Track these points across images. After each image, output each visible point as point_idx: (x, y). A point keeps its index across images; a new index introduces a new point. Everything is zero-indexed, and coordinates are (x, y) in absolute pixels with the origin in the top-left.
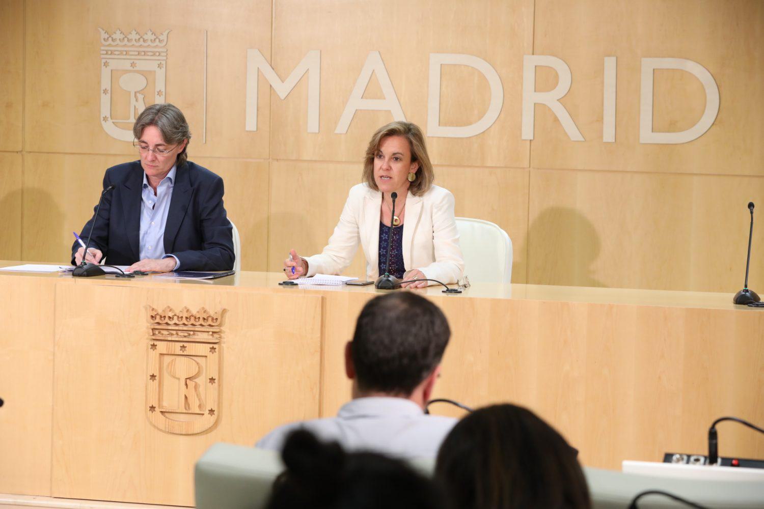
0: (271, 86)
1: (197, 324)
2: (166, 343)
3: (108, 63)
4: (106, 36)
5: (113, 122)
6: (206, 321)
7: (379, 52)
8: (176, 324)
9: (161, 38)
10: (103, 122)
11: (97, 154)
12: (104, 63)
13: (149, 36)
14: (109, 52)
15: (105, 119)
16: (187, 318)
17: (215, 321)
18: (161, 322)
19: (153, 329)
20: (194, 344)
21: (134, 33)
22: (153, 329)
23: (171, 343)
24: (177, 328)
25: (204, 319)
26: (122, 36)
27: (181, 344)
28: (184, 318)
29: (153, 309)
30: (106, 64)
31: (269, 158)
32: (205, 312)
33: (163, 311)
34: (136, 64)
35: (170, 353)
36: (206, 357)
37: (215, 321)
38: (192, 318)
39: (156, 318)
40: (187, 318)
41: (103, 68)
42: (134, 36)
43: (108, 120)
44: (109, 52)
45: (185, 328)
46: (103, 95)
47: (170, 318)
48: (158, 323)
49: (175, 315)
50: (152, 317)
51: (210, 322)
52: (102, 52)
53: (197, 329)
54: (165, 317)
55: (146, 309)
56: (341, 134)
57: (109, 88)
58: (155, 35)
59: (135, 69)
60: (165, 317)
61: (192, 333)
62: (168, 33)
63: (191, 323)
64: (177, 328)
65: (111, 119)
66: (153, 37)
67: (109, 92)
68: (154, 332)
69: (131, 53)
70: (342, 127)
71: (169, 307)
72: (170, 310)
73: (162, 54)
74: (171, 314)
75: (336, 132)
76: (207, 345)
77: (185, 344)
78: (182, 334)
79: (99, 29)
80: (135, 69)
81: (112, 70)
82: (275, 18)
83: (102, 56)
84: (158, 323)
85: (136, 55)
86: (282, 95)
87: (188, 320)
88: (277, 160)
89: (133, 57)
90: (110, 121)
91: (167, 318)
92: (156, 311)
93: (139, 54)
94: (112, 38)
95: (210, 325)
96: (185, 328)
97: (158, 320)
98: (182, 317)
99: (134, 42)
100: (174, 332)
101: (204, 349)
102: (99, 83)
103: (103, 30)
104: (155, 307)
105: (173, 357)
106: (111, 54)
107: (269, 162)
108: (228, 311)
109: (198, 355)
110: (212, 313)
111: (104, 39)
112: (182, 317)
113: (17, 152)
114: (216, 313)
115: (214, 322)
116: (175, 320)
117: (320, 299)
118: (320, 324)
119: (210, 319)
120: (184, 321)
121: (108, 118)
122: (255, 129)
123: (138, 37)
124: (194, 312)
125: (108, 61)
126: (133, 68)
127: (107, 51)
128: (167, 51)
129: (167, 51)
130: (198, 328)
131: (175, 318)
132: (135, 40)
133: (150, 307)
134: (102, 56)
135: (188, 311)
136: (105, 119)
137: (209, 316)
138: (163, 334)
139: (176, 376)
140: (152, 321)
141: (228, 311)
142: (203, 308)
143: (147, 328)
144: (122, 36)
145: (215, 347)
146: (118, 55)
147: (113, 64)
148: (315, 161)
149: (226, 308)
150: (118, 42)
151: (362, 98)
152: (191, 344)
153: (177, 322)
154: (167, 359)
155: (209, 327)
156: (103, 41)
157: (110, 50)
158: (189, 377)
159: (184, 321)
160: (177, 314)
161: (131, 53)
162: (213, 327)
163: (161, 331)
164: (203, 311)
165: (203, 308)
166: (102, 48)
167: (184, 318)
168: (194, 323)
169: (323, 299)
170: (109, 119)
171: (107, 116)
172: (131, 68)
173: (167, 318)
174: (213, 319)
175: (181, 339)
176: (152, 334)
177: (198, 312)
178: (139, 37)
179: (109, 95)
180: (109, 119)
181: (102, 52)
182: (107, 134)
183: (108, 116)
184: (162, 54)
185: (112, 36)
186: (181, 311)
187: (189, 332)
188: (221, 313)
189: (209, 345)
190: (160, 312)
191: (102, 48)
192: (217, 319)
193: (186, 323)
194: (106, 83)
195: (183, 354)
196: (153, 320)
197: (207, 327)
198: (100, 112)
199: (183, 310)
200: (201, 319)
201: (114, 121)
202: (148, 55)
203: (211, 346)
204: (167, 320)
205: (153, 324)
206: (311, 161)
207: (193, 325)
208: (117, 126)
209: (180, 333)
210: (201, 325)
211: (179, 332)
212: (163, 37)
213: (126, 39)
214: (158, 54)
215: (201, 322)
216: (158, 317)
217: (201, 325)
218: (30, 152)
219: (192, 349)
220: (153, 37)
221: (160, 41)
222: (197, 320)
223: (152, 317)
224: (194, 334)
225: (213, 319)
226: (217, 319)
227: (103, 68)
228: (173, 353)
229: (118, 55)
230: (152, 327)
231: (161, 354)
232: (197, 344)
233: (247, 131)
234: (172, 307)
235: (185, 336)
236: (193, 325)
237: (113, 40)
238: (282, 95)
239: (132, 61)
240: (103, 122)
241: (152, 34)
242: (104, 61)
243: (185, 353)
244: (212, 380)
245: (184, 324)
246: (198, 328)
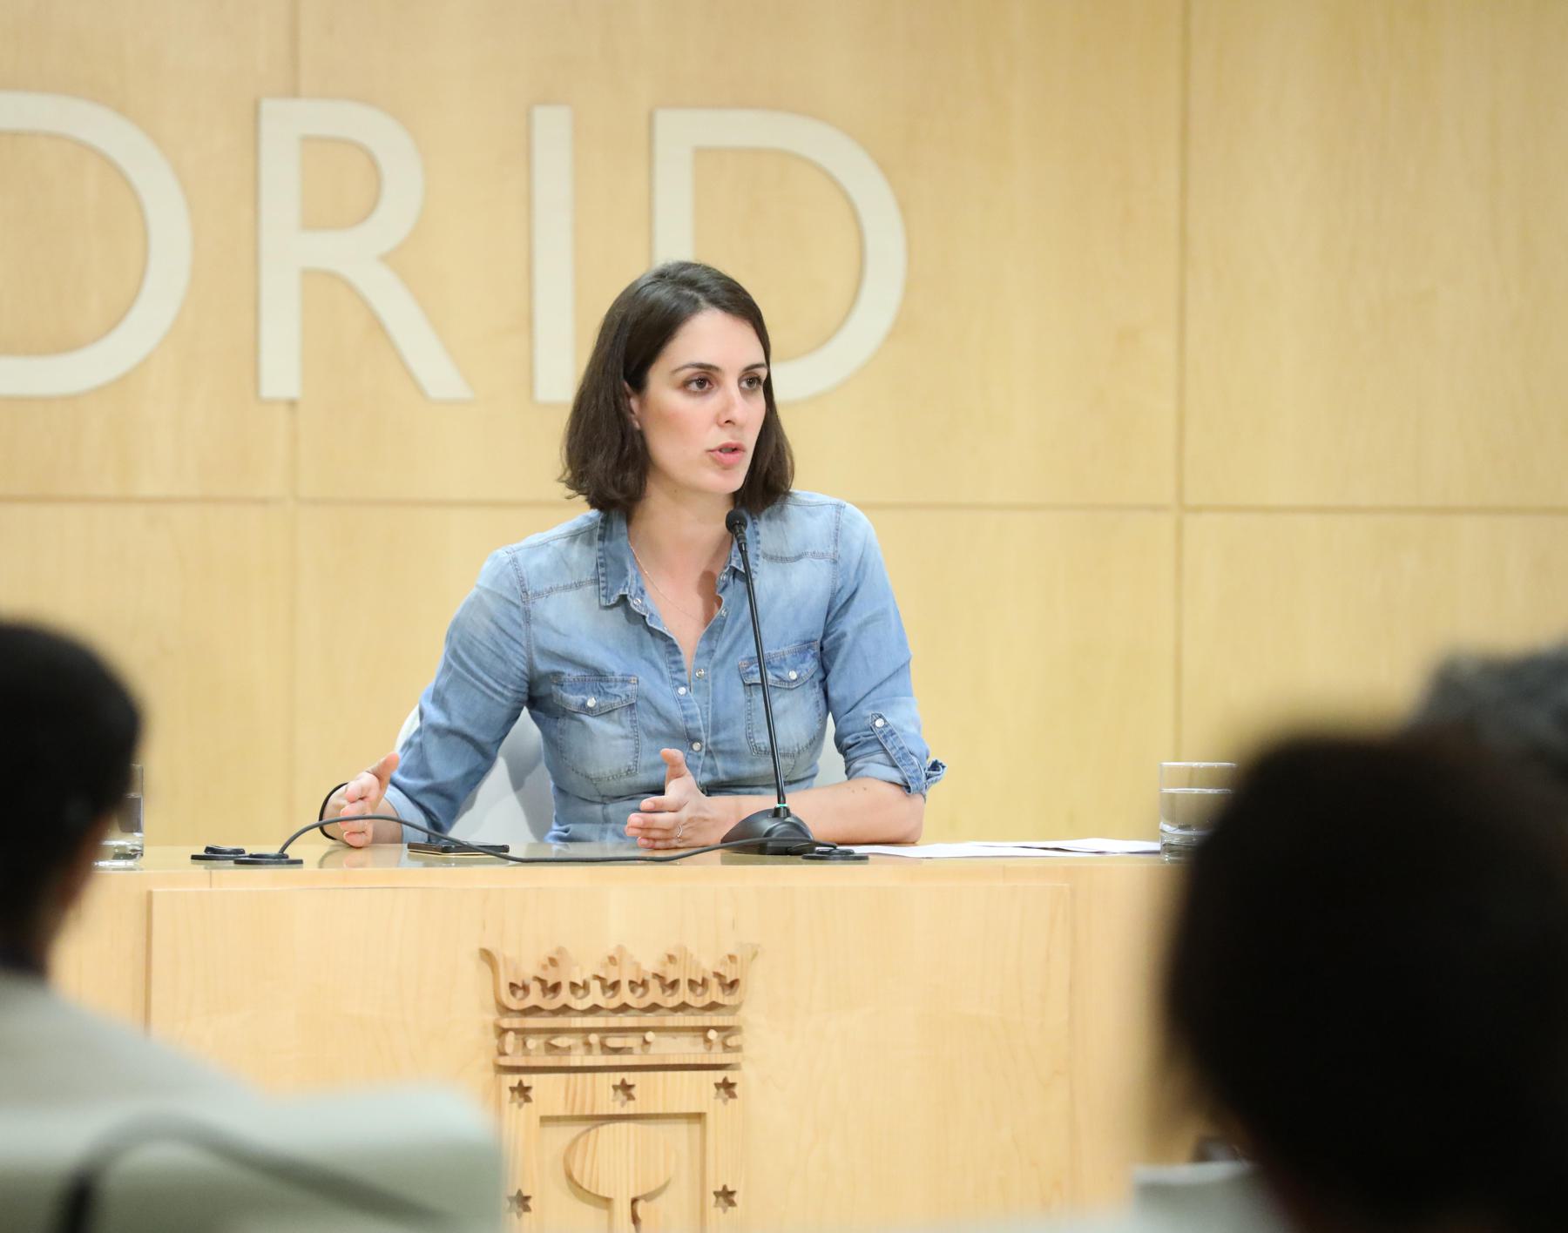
2: (563, 1076)
8: (595, 1010)
20: (660, 1074)
23: (580, 1076)
25: (692, 983)
27: (617, 1078)
28: (625, 987)
35: (577, 1112)
36: (699, 1117)
47: (573, 985)
76: (704, 1073)
77: (629, 1078)
78: (614, 1042)
84: (535, 1010)
97: (535, 997)
101: (693, 1091)
105: (576, 1129)
109: (676, 1110)
116: (596, 996)
120: (625, 995)
124: (650, 965)
139: (601, 1193)
145: (731, 1080)
152: (652, 1074)
154: (562, 1136)
158: (645, 1192)
175: (615, 1060)
189: (711, 1073)
190: (528, 970)
192: (733, 984)
195: (624, 1111)
200: (684, 986)
203: (719, 1076)
204: (565, 996)
209: (614, 1042)
219: (654, 1092)
226: (733, 984)
228: (587, 1112)
230: (516, 1022)
231: (546, 1120)
232: (670, 1074)
235: (617, 1051)
243: (630, 1108)
244: (726, 1196)
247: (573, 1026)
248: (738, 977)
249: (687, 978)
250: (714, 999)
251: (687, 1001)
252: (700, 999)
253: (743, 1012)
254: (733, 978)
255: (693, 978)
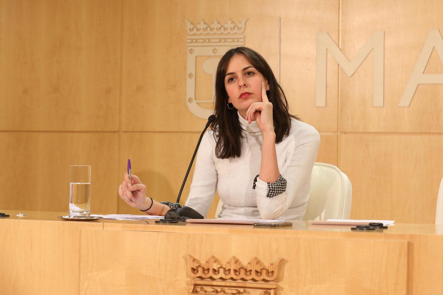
0: (339, 65)
1: (248, 278)
3: (193, 50)
4: (192, 26)
5: (197, 103)
6: (259, 274)
7: (439, 30)
8: (221, 279)
9: (240, 26)
10: (188, 103)
11: (183, 132)
12: (190, 50)
13: (229, 25)
14: (194, 41)
15: (190, 100)
16: (235, 271)
17: (270, 274)
18: (203, 276)
19: (195, 285)
21: (216, 22)
22: (195, 285)
24: (223, 283)
25: (257, 272)
26: (205, 26)
28: (232, 272)
29: (194, 260)
30: (191, 51)
31: (338, 132)
32: (258, 262)
33: (207, 262)
34: (217, 50)
37: (270, 274)
38: (242, 271)
39: (198, 272)
40: (235, 271)
41: (189, 55)
42: (216, 25)
43: (192, 101)
44: (194, 41)
45: (234, 284)
46: (188, 79)
47: (214, 271)
48: (201, 278)
49: (221, 267)
50: (193, 270)
51: (264, 276)
52: (188, 41)
53: (248, 285)
54: (209, 269)
55: (186, 260)
56: (404, 107)
57: (193, 73)
58: (234, 24)
59: (217, 54)
60: (209, 269)
61: (242, 290)
62: (247, 21)
63: (240, 277)
64: (223, 283)
65: (196, 99)
66: (232, 26)
67: (194, 76)
68: (204, 290)
69: (213, 40)
70: (405, 101)
71: (213, 257)
72: (216, 261)
73: (241, 40)
74: (216, 266)
75: (400, 105)
79: (186, 21)
80: (217, 54)
81: (196, 57)
82: (342, 20)
83: (188, 45)
84: (201, 278)
85: (218, 42)
86: (349, 73)
87: (237, 273)
88: (345, 133)
89: (215, 44)
90: (194, 102)
91: (211, 271)
92: (198, 262)
93: (220, 41)
94: (197, 28)
95: (264, 280)
96: (234, 284)
97: (200, 274)
98: (229, 270)
99: (215, 31)
100: (219, 289)
102: (185, 68)
103: (189, 21)
104: (196, 257)
106: (196, 42)
107: (338, 136)
108: (288, 261)
110: (267, 265)
111: (190, 29)
112: (229, 270)
113: (114, 132)
114: (272, 264)
115: (269, 276)
116: (222, 274)
117: (406, 245)
118: (405, 279)
119: (264, 272)
120: (233, 275)
121: (193, 99)
122: (325, 105)
123: (219, 26)
124: (245, 263)
125: (193, 48)
126: (215, 53)
127: (192, 39)
128: (245, 37)
129: (245, 37)
130: (250, 284)
131: (221, 271)
132: (217, 29)
133: (191, 257)
134: (188, 45)
135: (237, 261)
136: (190, 100)
137: (263, 269)
138: (206, 291)
140: (193, 275)
141: (288, 261)
142: (256, 258)
143: (188, 284)
144: (205, 26)
146: (202, 42)
147: (198, 51)
148: (381, 133)
149: (285, 257)
150: (201, 31)
151: (423, 73)
153: (224, 276)
155: (263, 282)
156: (189, 32)
157: (195, 39)
159: (233, 275)
160: (224, 266)
161: (213, 40)
162: (269, 283)
163: (204, 287)
164: (255, 262)
165: (256, 258)
166: (188, 37)
167: (232, 272)
168: (245, 277)
169: (410, 246)
170: (194, 100)
171: (192, 98)
172: (213, 54)
173: (211, 271)
174: (268, 272)
176: (191, 291)
177: (249, 263)
178: (221, 26)
179: (193, 79)
180: (194, 100)
181: (188, 41)
182: (192, 114)
183: (193, 97)
184: (241, 40)
185: (197, 26)
186: (228, 263)
187: (239, 289)
188: (278, 263)
190: (203, 263)
191: (188, 37)
192: (273, 272)
193: (235, 277)
194: (191, 69)
196: (194, 273)
197: (261, 282)
198: (185, 93)
199: (231, 260)
200: (253, 272)
201: (198, 101)
202: (228, 42)
204: (211, 274)
205: (194, 278)
206: (376, 133)
207: (243, 279)
208: (199, 105)
210: (253, 280)
211: (226, 289)
212: (242, 25)
213: (209, 29)
214: (236, 40)
215: (253, 275)
216: (200, 270)
217: (253, 280)
218: (126, 132)
220: (233, 26)
221: (238, 29)
222: (248, 273)
223: (193, 270)
224: (245, 292)
225: (268, 272)
226: (273, 272)
227: (189, 55)
229: (202, 42)
233: (317, 107)
234: (216, 256)
236: (243, 279)
237: (198, 30)
238: (349, 73)
239: (213, 48)
240: (188, 103)
241: (232, 23)
242: (190, 48)
245: (232, 279)
246: (250, 284)
247: (213, 284)
248: (273, 270)
249: (254, 269)
250: (264, 278)
251: (254, 278)
252: (259, 277)
253: (281, 284)
254: (271, 270)
255: (257, 270)
